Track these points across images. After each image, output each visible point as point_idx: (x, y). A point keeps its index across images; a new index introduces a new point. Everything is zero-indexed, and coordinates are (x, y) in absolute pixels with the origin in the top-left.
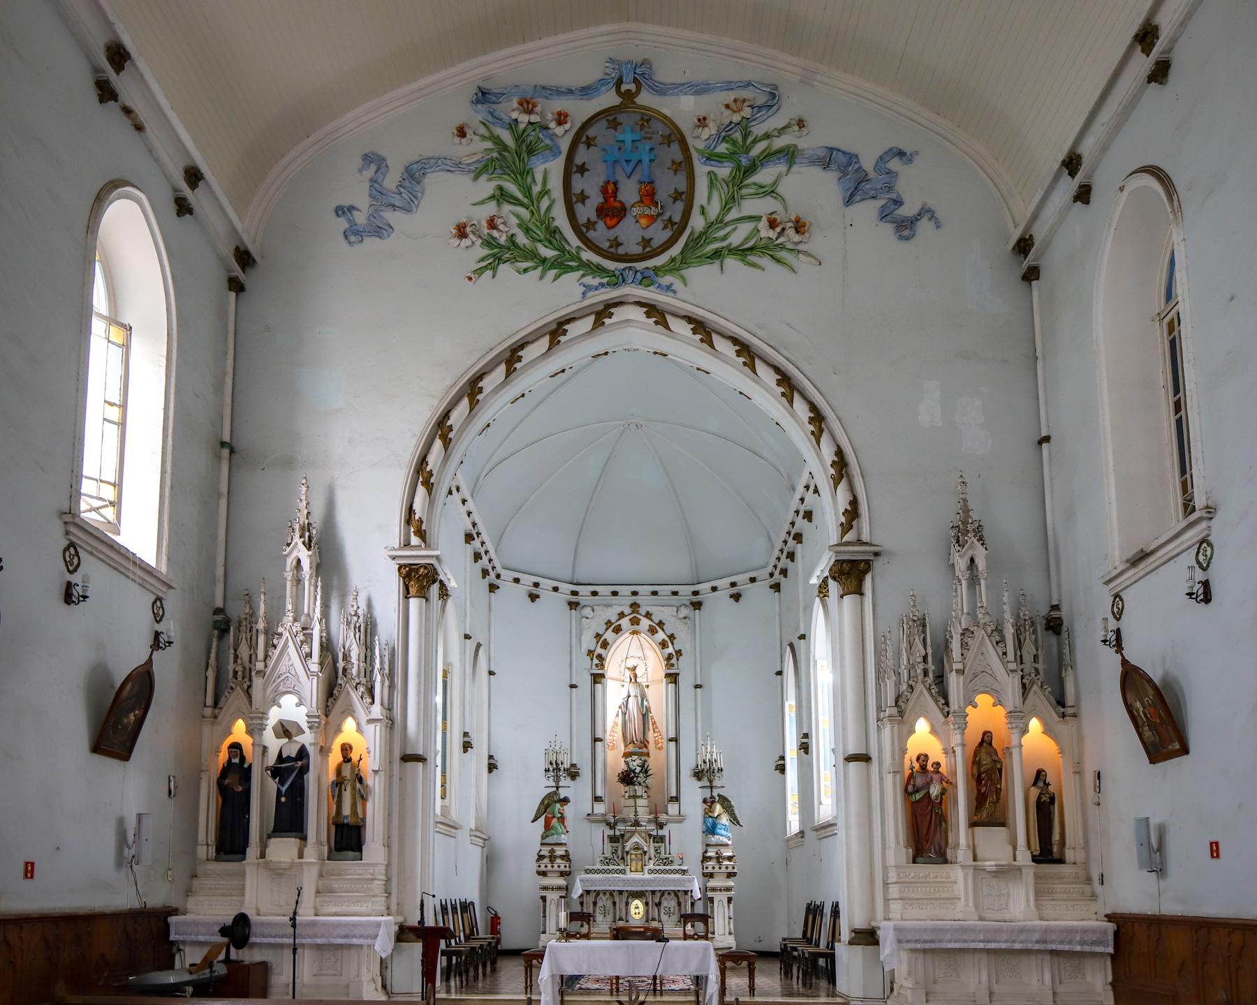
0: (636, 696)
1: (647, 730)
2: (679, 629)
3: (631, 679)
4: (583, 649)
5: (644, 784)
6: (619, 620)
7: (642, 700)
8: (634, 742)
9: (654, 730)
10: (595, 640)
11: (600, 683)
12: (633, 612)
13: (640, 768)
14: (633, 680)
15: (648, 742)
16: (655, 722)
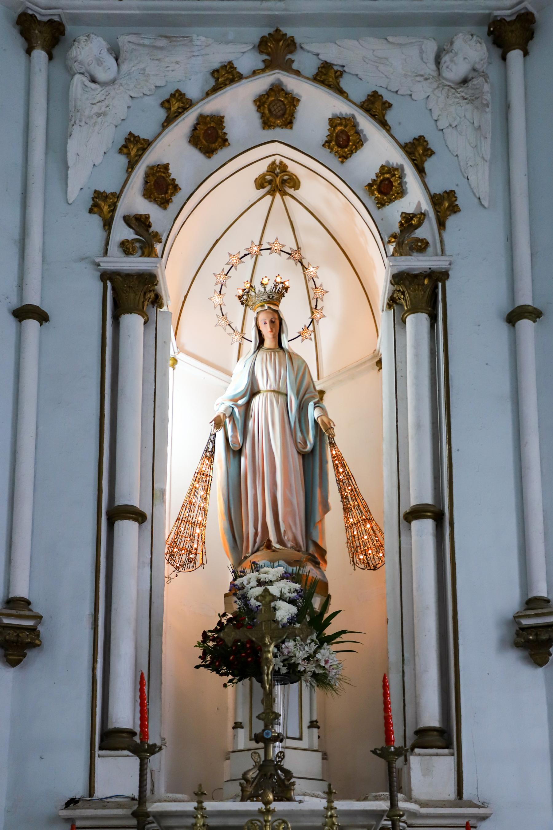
0: (280, 393)
1: (318, 508)
2: (442, 124)
3: (262, 341)
4: (73, 192)
5: (311, 668)
6: (215, 89)
7: (302, 409)
8: (269, 546)
9: (344, 498)
10: (123, 160)
11: (142, 313)
12: (269, 66)
13: (293, 610)
14: (269, 342)
15: (323, 552)
16: (349, 477)
